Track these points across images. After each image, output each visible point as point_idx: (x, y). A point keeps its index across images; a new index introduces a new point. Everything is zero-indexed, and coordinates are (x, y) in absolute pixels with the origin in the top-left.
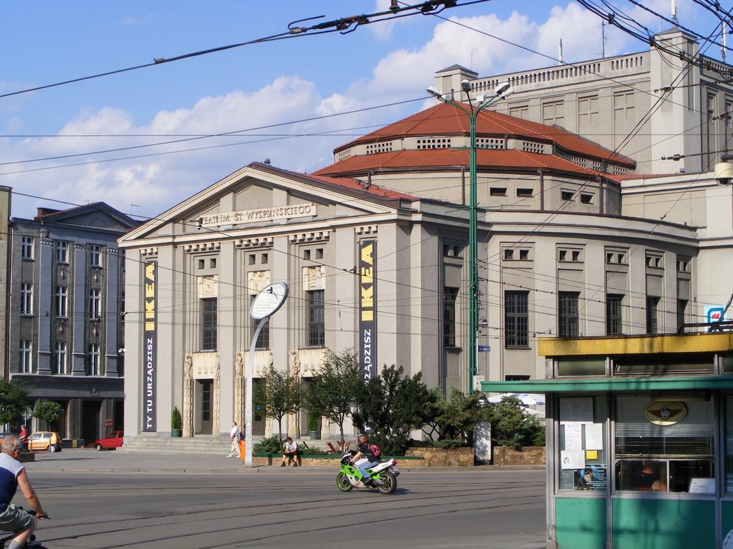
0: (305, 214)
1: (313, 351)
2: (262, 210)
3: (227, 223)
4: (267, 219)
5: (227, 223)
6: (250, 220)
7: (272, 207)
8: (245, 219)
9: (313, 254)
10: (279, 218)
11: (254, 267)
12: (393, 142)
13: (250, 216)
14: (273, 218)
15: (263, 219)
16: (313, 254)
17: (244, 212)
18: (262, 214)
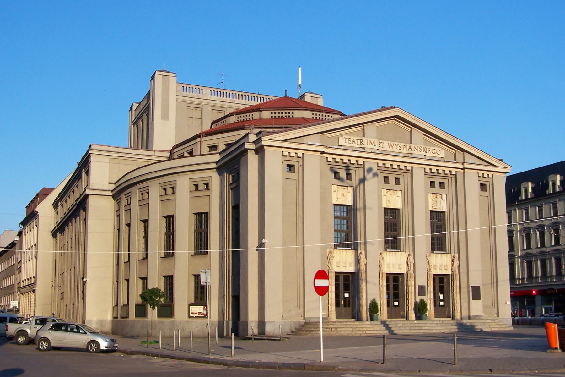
0: (436, 155)
1: (440, 255)
2: (402, 144)
3: (372, 147)
4: (405, 151)
5: (372, 147)
6: (391, 149)
7: (411, 143)
8: (386, 147)
9: (437, 185)
10: (421, 153)
11: (386, 186)
12: (295, 112)
13: (391, 146)
14: (412, 152)
15: (402, 151)
16: (437, 185)
17: (386, 142)
18: (402, 147)
